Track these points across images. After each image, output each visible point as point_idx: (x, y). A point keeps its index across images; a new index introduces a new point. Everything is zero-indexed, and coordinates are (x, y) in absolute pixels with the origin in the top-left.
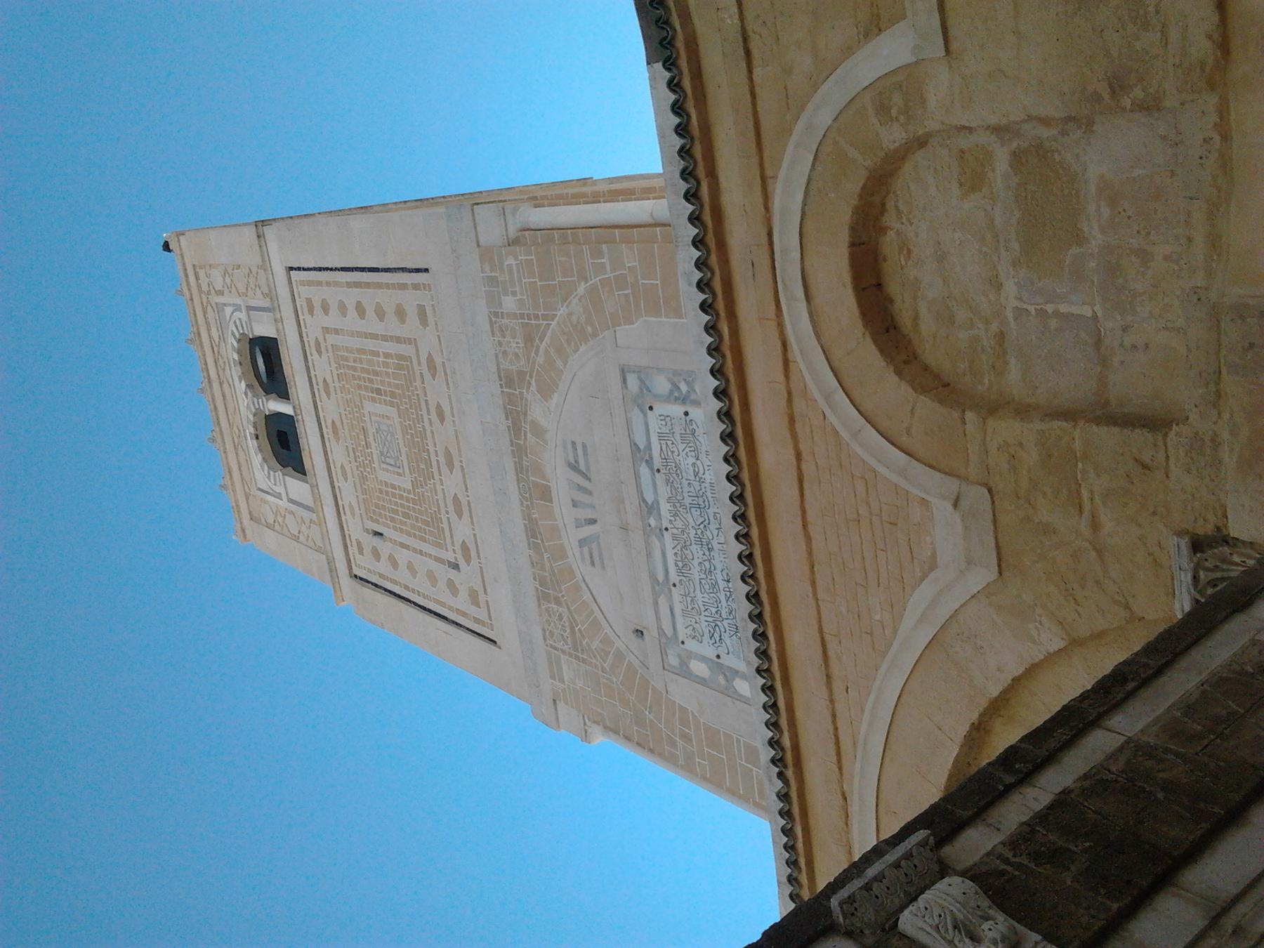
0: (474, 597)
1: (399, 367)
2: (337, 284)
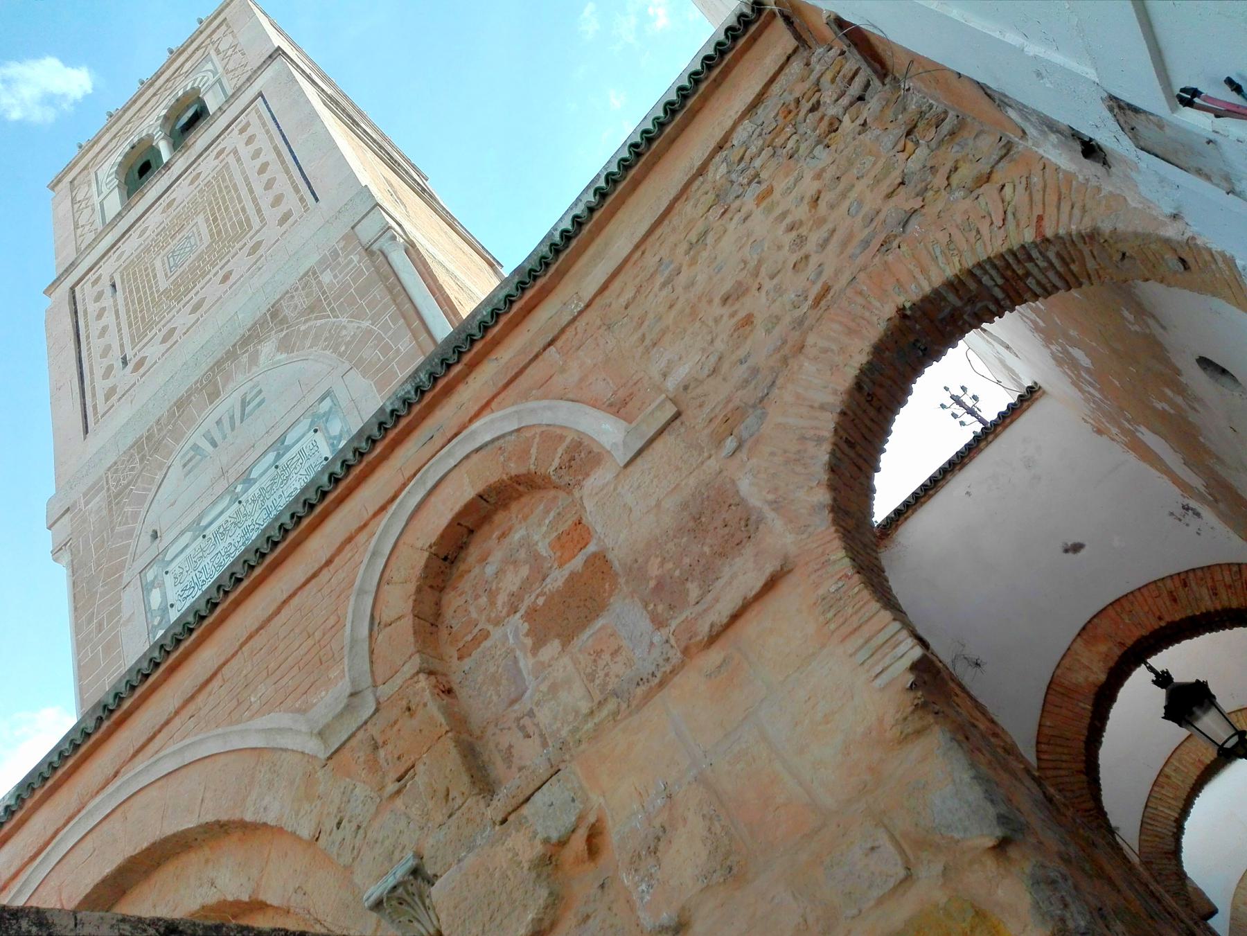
1: (240, 223)
2: (271, 139)
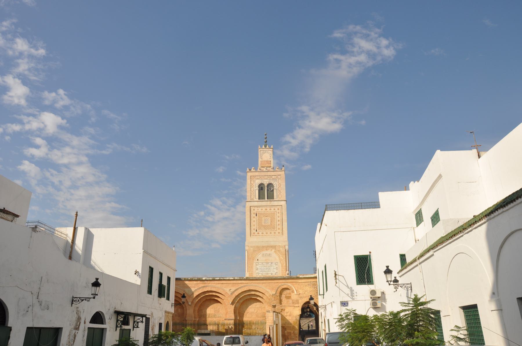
0: (254, 233)
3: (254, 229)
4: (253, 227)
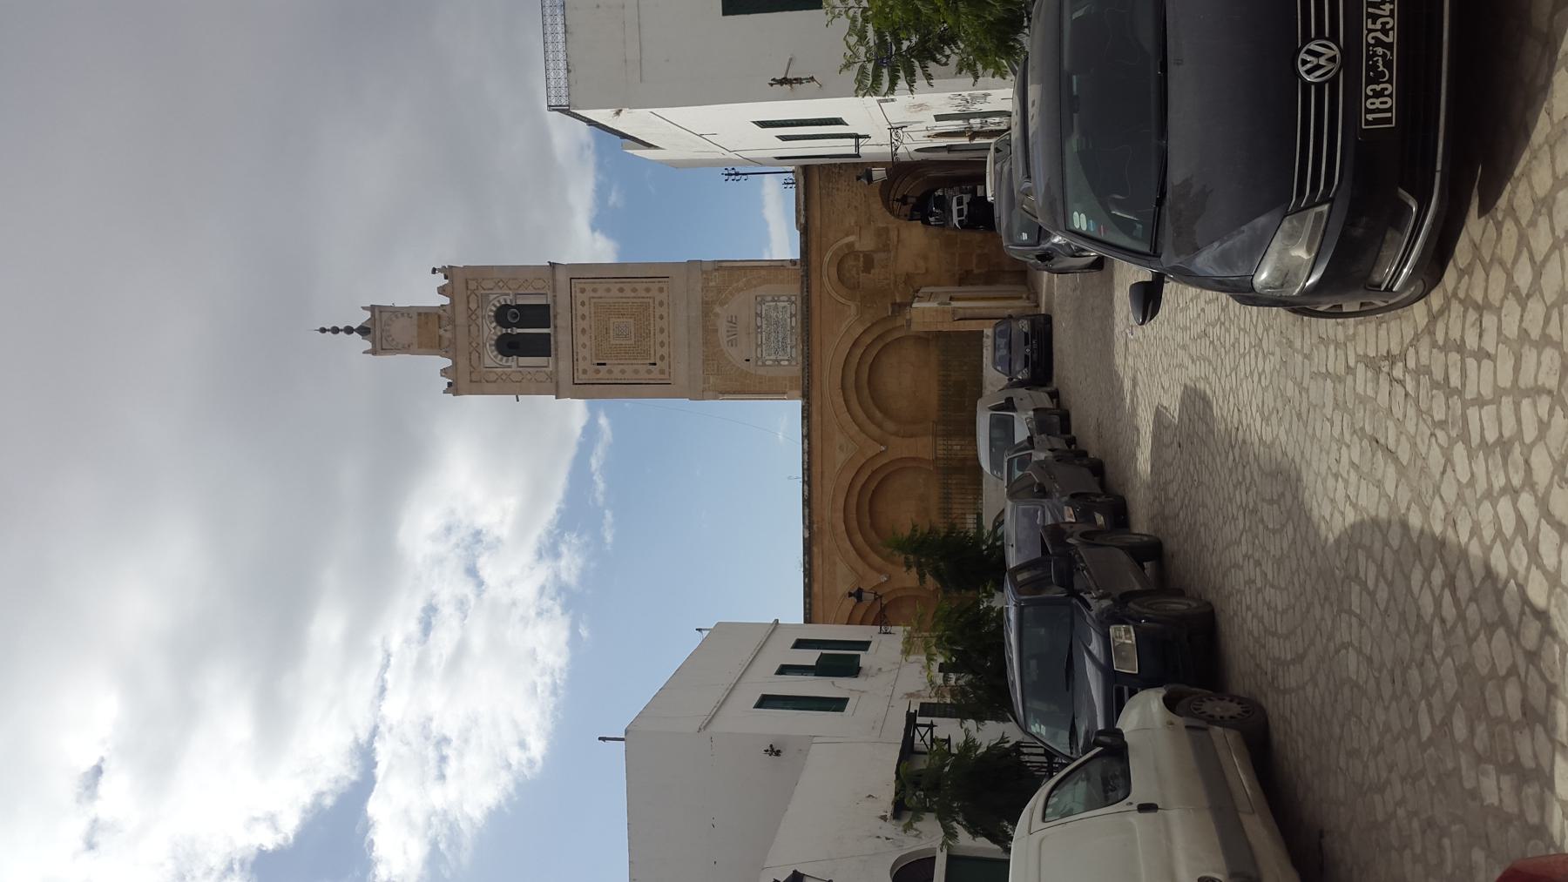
0: (662, 372)
3: (649, 372)
4: (643, 376)
